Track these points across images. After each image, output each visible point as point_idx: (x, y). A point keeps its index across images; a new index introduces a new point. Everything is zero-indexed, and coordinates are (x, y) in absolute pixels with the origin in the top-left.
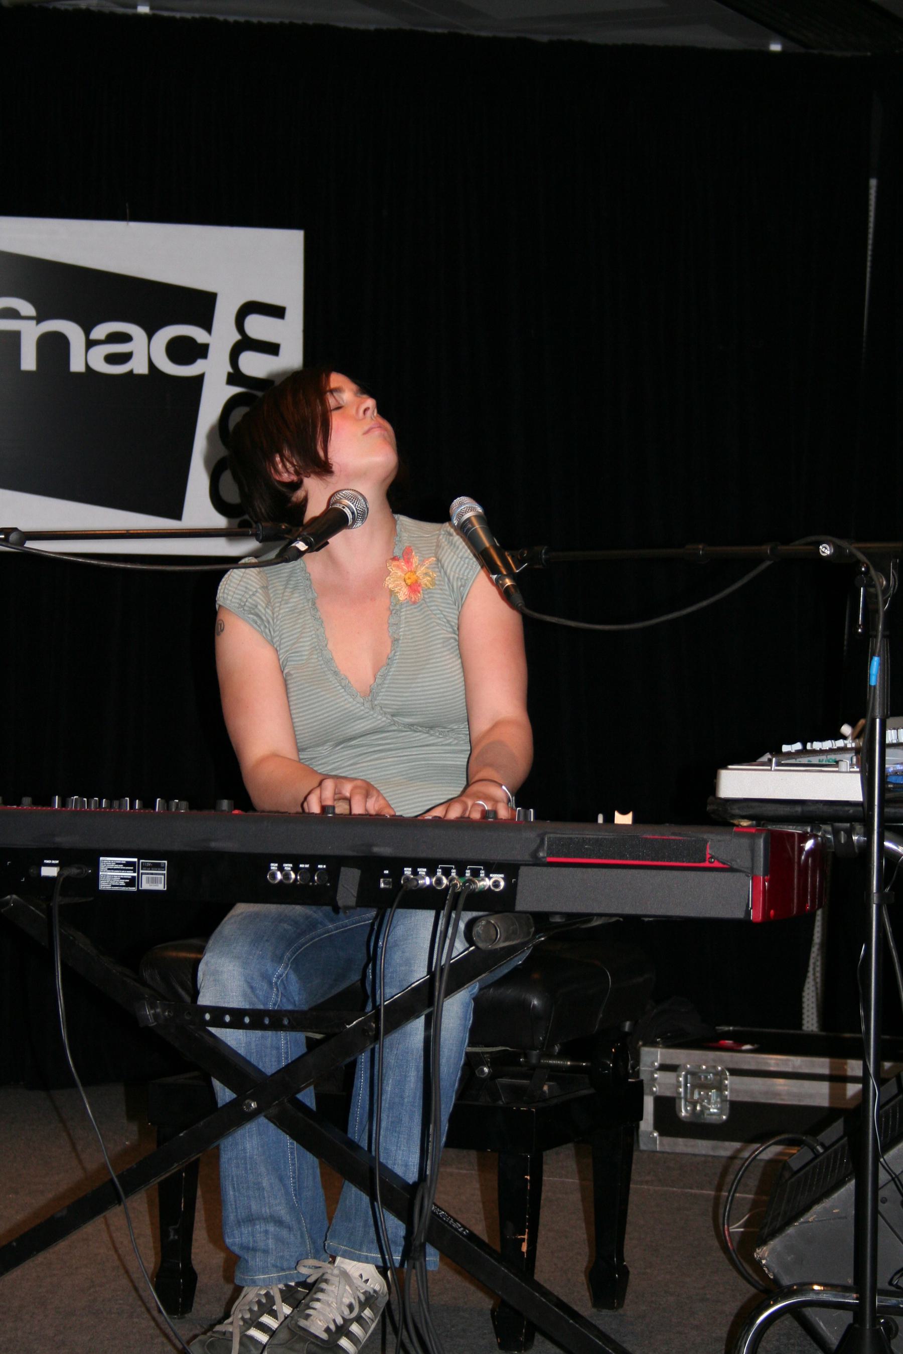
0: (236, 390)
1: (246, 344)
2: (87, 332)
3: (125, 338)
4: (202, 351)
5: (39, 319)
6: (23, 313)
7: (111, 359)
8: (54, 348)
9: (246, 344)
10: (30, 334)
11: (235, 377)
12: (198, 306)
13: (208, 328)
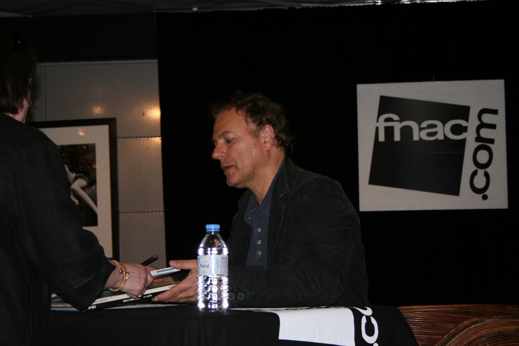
0: (478, 144)
1: (482, 125)
2: (419, 124)
3: (435, 126)
4: (465, 129)
5: (401, 121)
7: (429, 135)
8: (406, 132)
9: (482, 125)
10: (397, 127)
11: (479, 139)
12: (463, 112)
13: (467, 120)
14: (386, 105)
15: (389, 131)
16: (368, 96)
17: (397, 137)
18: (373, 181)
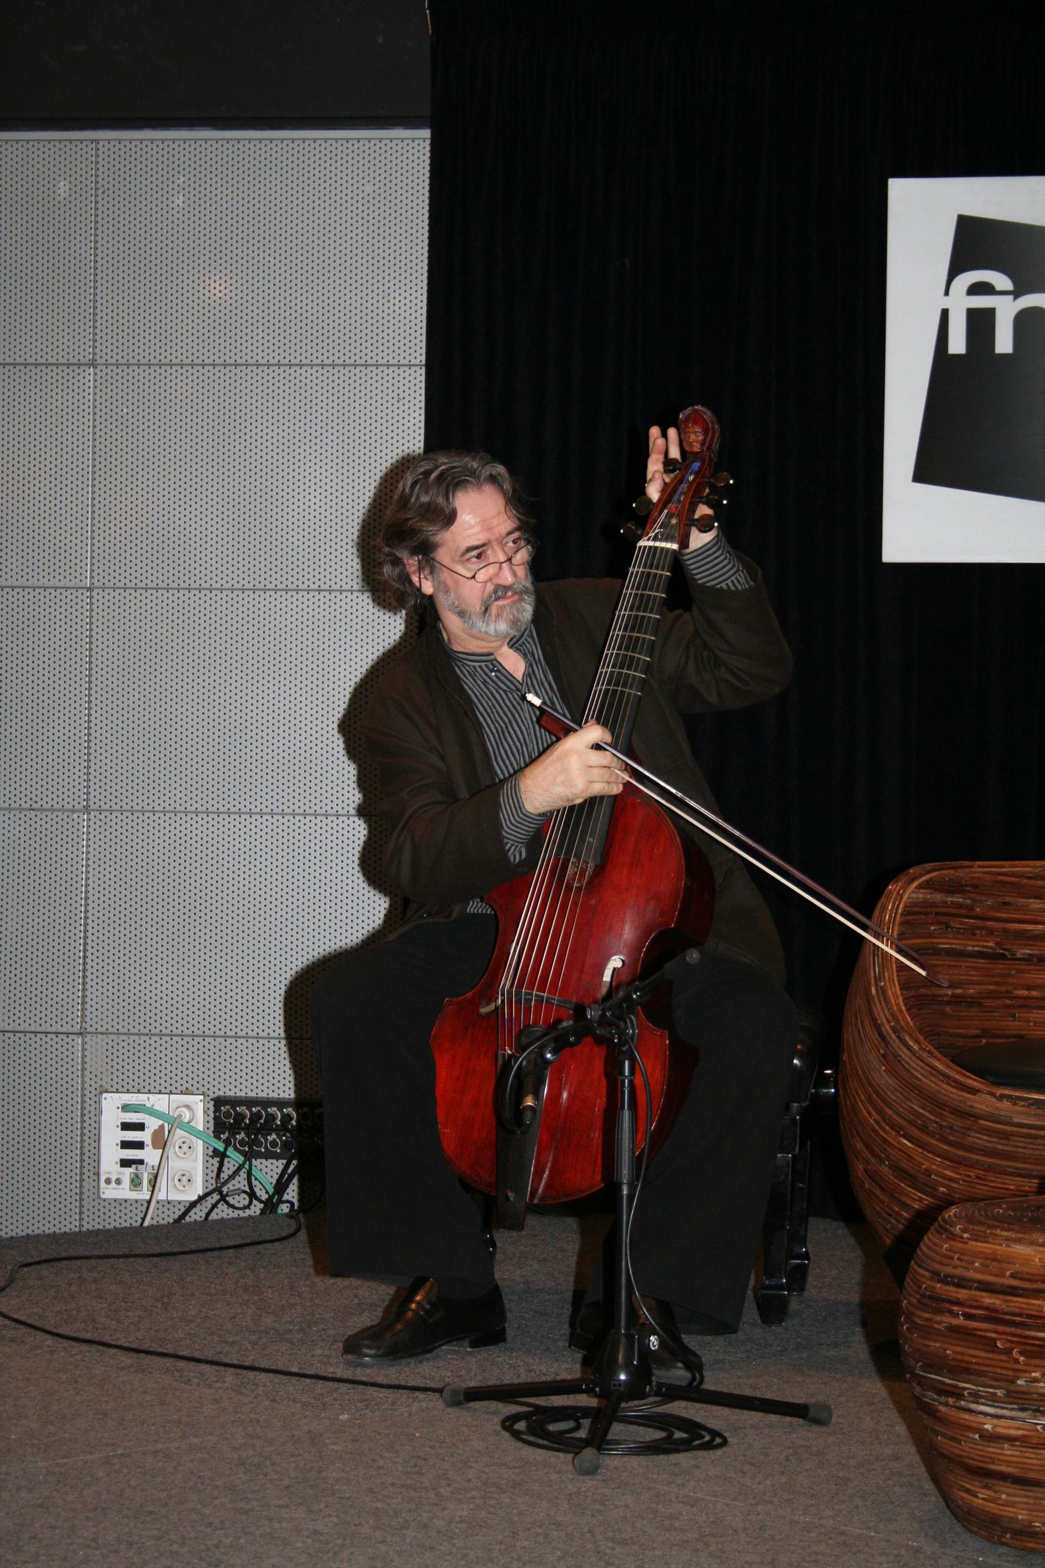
5: (1017, 293)
6: (999, 287)
10: (1006, 311)
14: (977, 244)
15: (981, 323)
16: (922, 214)
17: (1004, 343)
18: (924, 473)
